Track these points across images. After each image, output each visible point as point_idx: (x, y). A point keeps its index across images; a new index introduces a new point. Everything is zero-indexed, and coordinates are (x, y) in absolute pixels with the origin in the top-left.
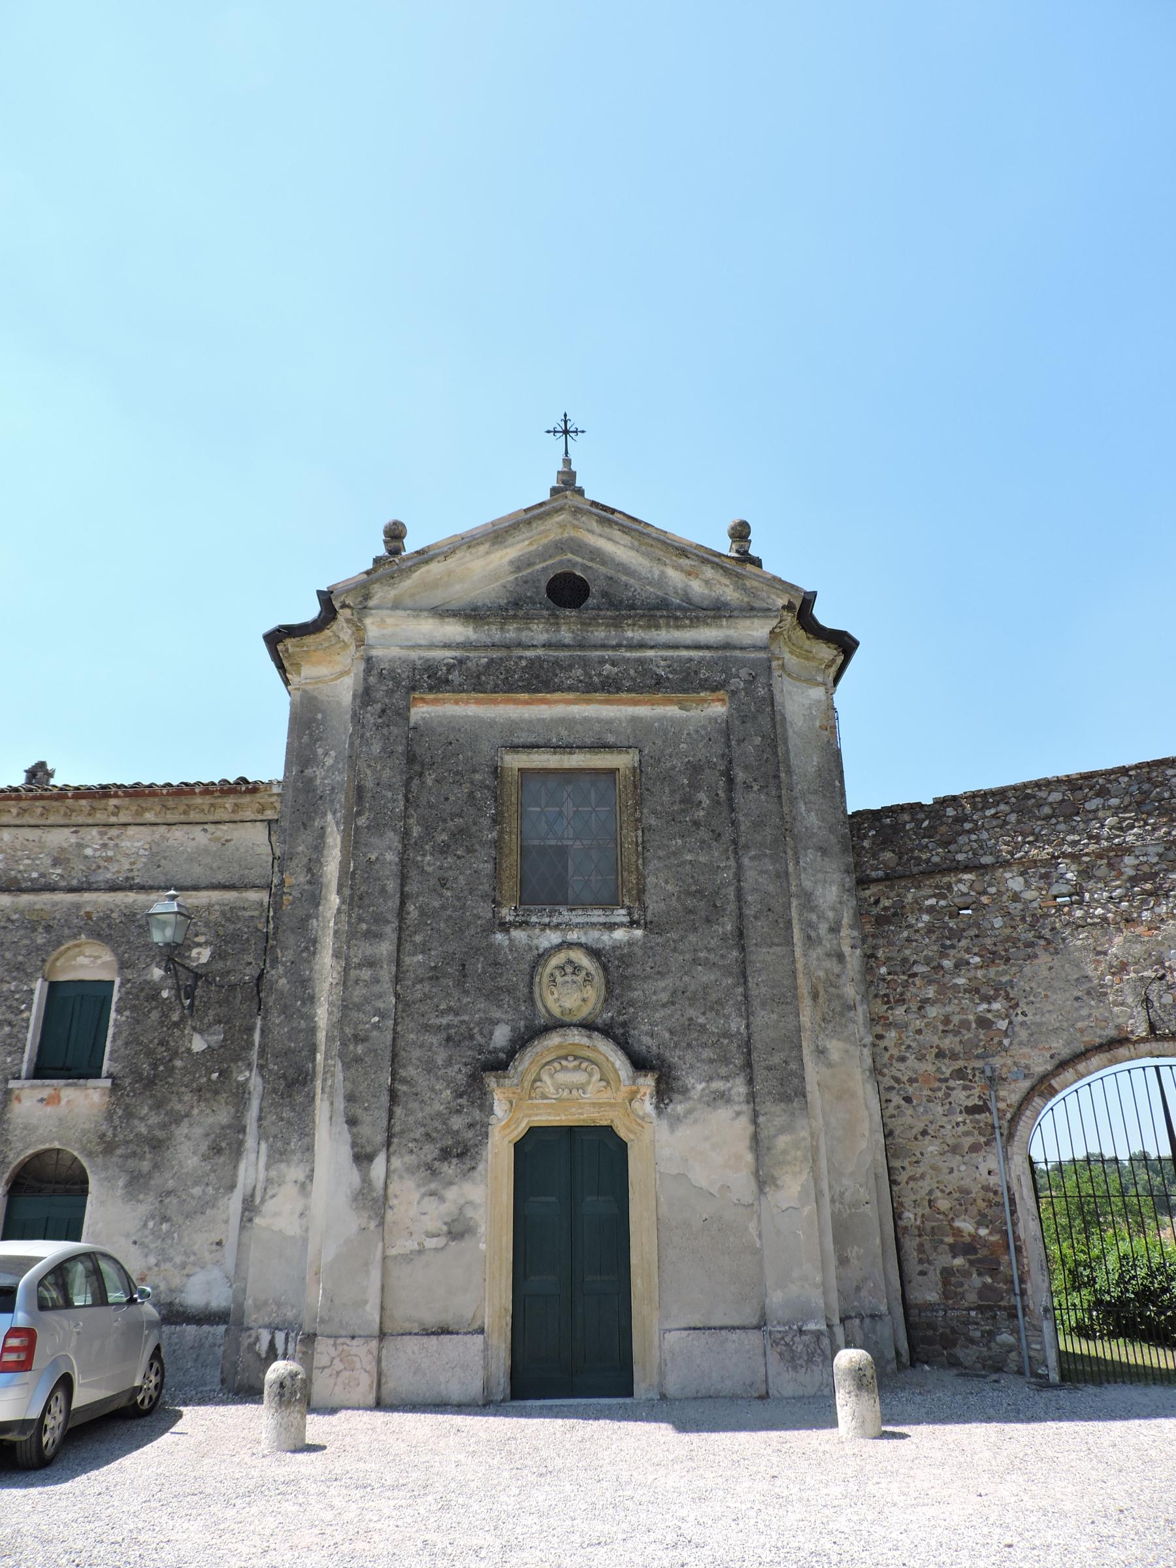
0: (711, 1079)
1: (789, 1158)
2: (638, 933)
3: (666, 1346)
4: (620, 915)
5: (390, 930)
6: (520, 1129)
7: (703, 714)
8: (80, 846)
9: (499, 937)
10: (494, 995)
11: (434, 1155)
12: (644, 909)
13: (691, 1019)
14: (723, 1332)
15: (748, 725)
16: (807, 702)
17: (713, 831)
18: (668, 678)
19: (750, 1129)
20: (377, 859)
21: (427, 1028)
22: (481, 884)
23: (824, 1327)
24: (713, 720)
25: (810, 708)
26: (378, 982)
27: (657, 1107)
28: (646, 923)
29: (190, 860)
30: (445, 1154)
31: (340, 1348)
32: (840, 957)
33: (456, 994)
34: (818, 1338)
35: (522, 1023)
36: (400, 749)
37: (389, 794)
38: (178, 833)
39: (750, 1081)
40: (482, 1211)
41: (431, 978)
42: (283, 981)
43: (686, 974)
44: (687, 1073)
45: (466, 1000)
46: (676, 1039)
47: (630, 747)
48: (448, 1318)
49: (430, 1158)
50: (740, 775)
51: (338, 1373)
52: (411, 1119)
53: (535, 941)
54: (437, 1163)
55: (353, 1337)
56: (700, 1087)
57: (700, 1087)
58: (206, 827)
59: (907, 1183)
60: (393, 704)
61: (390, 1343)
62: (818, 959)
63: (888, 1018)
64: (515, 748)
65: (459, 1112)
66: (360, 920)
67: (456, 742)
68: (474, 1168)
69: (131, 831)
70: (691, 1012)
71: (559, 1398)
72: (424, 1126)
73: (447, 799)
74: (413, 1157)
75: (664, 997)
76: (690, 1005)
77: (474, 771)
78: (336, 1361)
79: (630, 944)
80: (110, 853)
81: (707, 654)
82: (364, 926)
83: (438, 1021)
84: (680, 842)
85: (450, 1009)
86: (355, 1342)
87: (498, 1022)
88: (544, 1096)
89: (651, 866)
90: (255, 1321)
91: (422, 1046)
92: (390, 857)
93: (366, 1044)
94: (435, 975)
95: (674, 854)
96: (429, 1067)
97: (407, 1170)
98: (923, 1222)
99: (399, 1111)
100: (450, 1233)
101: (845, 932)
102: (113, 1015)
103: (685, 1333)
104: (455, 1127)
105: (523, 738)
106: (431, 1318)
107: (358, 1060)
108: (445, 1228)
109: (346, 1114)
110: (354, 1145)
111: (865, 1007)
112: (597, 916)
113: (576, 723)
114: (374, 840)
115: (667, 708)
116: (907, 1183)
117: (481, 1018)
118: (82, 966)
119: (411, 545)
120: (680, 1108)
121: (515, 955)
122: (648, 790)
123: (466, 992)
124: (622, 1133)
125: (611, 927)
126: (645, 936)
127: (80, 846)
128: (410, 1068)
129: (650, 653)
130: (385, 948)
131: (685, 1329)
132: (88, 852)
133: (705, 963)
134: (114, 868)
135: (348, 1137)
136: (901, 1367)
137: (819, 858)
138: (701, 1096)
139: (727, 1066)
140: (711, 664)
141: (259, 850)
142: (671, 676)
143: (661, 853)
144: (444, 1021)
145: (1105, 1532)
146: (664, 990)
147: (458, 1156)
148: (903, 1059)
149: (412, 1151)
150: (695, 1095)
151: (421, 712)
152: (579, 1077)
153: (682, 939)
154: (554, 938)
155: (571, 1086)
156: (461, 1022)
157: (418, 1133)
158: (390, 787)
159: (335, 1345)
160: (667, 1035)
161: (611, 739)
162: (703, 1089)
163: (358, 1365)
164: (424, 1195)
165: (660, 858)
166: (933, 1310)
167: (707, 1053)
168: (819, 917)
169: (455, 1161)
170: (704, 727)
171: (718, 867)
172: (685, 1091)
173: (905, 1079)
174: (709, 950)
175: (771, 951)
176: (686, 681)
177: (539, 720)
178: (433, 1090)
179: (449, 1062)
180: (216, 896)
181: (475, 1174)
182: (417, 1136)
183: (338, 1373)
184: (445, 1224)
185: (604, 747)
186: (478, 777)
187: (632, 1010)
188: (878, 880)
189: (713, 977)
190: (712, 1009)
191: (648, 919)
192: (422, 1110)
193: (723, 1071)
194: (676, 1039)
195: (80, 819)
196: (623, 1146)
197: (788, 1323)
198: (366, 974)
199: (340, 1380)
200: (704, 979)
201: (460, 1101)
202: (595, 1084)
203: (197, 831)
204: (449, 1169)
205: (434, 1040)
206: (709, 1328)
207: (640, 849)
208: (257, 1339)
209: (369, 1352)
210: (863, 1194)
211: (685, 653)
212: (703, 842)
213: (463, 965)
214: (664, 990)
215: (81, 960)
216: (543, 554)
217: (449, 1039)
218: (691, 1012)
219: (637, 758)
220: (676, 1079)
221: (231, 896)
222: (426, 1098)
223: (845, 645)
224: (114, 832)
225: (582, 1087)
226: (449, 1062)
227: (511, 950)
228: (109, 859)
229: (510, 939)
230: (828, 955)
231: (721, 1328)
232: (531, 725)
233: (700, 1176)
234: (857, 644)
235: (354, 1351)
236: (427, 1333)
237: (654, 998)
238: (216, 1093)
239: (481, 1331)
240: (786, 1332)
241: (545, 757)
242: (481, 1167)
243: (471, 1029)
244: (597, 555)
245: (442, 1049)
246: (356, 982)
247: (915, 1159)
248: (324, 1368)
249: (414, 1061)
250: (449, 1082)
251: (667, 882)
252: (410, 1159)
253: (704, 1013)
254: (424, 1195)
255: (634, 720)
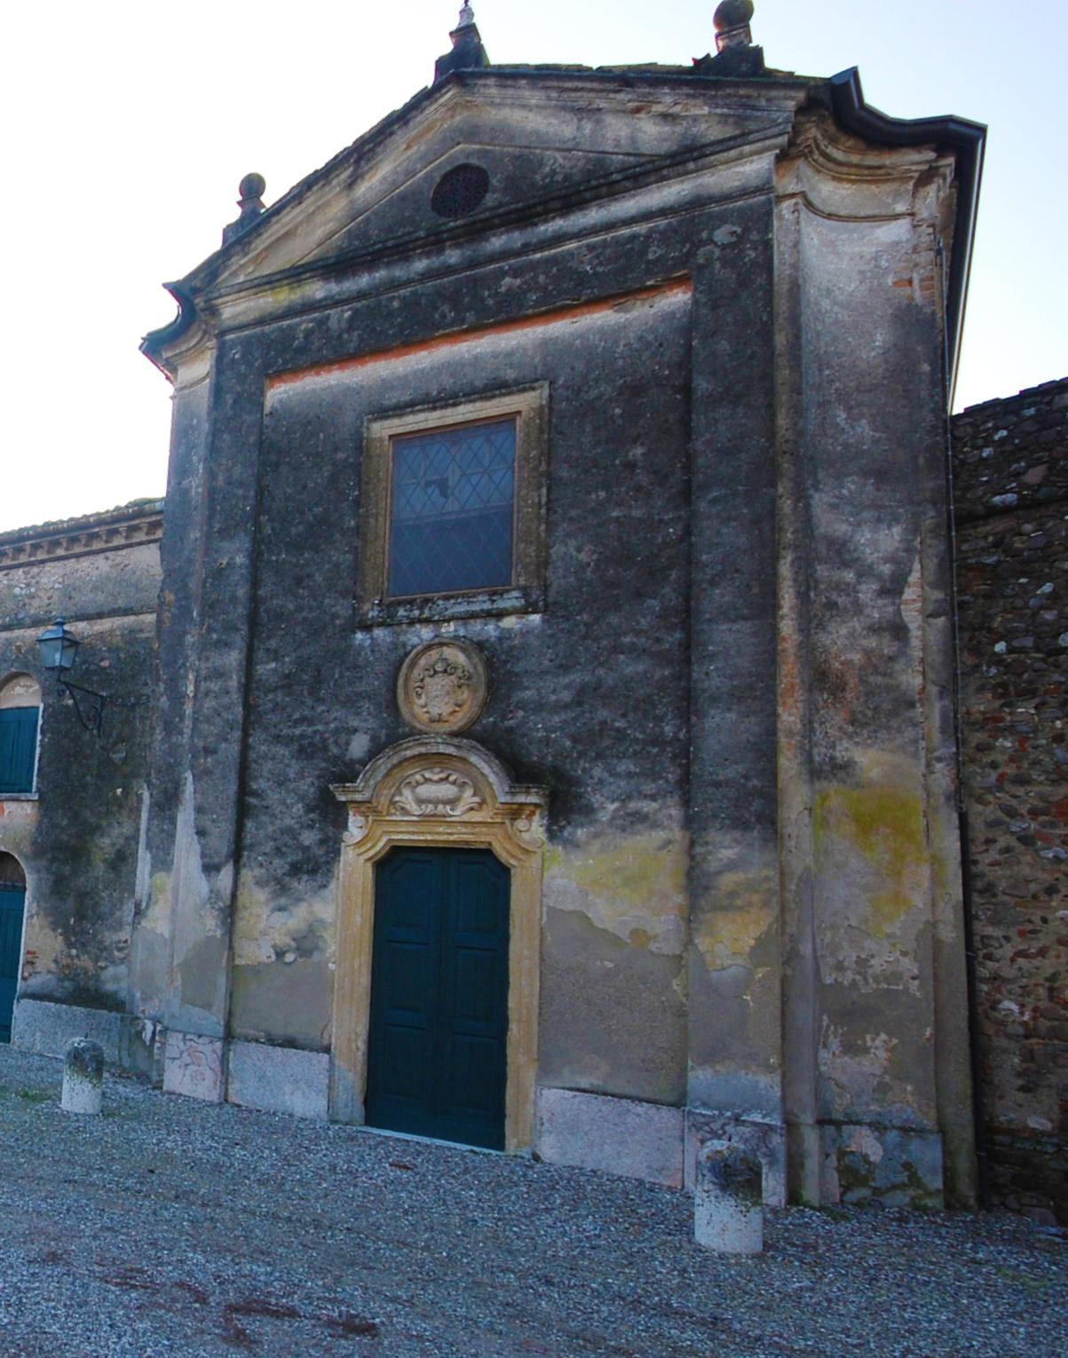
0: (629, 797)
1: (739, 902)
2: (536, 618)
3: (542, 1103)
4: (512, 600)
5: (239, 640)
6: (377, 848)
7: (652, 311)
8: (10, 587)
9: (359, 636)
10: (351, 703)
11: (284, 871)
12: (546, 588)
13: (603, 723)
14: (624, 1102)
15: (721, 311)
16: (869, 251)
17: (655, 472)
18: (596, 274)
19: (684, 862)
20: (228, 564)
21: (278, 738)
22: (340, 578)
23: (776, 1121)
24: (668, 317)
25: (876, 258)
26: (228, 692)
27: (549, 830)
28: (546, 606)
29: (95, 589)
30: (295, 870)
31: (189, 1043)
32: (898, 630)
33: (310, 702)
34: (765, 1134)
35: (384, 731)
36: (252, 439)
37: (240, 492)
38: (85, 563)
39: (686, 802)
40: (331, 931)
41: (282, 687)
42: (164, 699)
43: (601, 664)
44: (594, 790)
45: (320, 709)
46: (580, 747)
47: (537, 380)
48: (292, 1031)
49: (280, 872)
50: (702, 385)
51: (187, 1065)
52: (262, 833)
53: (402, 638)
54: (287, 879)
55: (200, 1036)
56: (612, 807)
57: (612, 807)
58: (108, 554)
59: (1013, 960)
60: (245, 391)
61: (238, 1048)
62: (852, 634)
63: (1002, 720)
64: (384, 413)
65: (311, 827)
66: (210, 630)
67: (310, 420)
68: (325, 886)
69: (48, 567)
70: (603, 714)
71: (455, 1141)
72: (275, 840)
73: (305, 487)
74: (263, 871)
75: (566, 696)
76: (604, 705)
77: (336, 449)
78: (185, 1054)
79: (524, 633)
80: (33, 590)
81: (662, 223)
82: (215, 636)
83: (290, 732)
84: (602, 494)
85: (303, 720)
86: (201, 1040)
87: (355, 731)
88: (405, 811)
89: (560, 532)
90: (143, 1012)
91: (273, 758)
92: (240, 559)
93: (215, 757)
94: (288, 682)
95: (592, 511)
96: (281, 782)
97: (257, 883)
98: (1034, 1018)
99: (249, 824)
100: (298, 949)
101: (910, 593)
102: (39, 737)
103: (569, 1094)
104: (307, 843)
105: (392, 398)
106: (279, 1031)
107: (208, 772)
108: (293, 944)
109: (197, 827)
110: (203, 855)
111: (946, 702)
112: (481, 604)
113: (463, 366)
114: (225, 544)
115: (596, 316)
116: (1013, 960)
117: (337, 728)
118: (19, 695)
119: (269, 199)
120: (581, 833)
121: (378, 655)
122: (561, 433)
123: (321, 700)
124: (503, 856)
125: (500, 615)
126: (544, 621)
127: (10, 587)
128: (261, 781)
129: (572, 245)
130: (234, 658)
131: (571, 1089)
132: (17, 591)
133: (631, 649)
134: (36, 603)
135: (197, 848)
136: (953, 1201)
137: (869, 488)
138: (613, 818)
139: (654, 781)
140: (664, 236)
141: (152, 571)
142: (600, 269)
143: (573, 513)
144: (297, 732)
145: (124, 1340)
146: (566, 687)
147: (308, 872)
148: (1022, 781)
149: (261, 865)
150: (604, 816)
151: (278, 393)
152: (447, 790)
153: (597, 620)
154: (426, 633)
155: (445, 804)
156: (315, 732)
157: (269, 847)
158: (241, 484)
159: (184, 1040)
160: (568, 743)
161: (511, 374)
162: (617, 810)
163: (204, 1062)
164: (273, 911)
165: (571, 519)
166: (1039, 1142)
167: (625, 766)
168: (860, 575)
169: (305, 877)
170: (652, 330)
171: (661, 521)
172: (589, 811)
173: (1024, 809)
174: (638, 633)
175: (735, 627)
176: (621, 275)
177: (415, 373)
178: (283, 803)
179: (301, 775)
180: (118, 622)
181: (326, 892)
182: (267, 850)
183: (187, 1065)
184: (294, 940)
185: (499, 387)
186: (341, 455)
187: (521, 713)
188: (1006, 510)
189: (641, 668)
190: (636, 709)
191: (550, 600)
192: (272, 823)
193: (649, 788)
194: (580, 747)
195: (9, 562)
196: (504, 872)
197: (721, 1108)
198: (215, 686)
199: (188, 1072)
200: (629, 670)
201: (312, 816)
202: (468, 797)
203: (100, 559)
204: (300, 885)
205: (281, 750)
206: (605, 1094)
207: (543, 511)
208: (144, 1028)
209: (214, 1051)
210: (909, 966)
211: (626, 231)
212: (638, 489)
213: (319, 671)
214: (566, 687)
215: (18, 690)
216: (426, 160)
217: (301, 750)
218: (603, 714)
219: (546, 392)
220: (581, 796)
221: (129, 620)
222: (277, 812)
223: (956, 144)
224: (35, 570)
225: (453, 802)
226: (301, 775)
227: (373, 651)
228: (32, 597)
229: (372, 638)
230: (874, 629)
231: (621, 1097)
232: (404, 381)
233: (605, 914)
234: (981, 130)
235: (200, 1048)
236: (272, 1041)
237: (553, 698)
238: (121, 806)
239: (327, 1050)
240: (713, 1116)
241: (422, 416)
242: (332, 886)
243: (326, 740)
244: (501, 132)
245: (294, 761)
246: (207, 694)
247: (1030, 927)
248: (174, 1059)
249: (265, 773)
250: (301, 798)
251: (579, 550)
252: (258, 872)
253: (624, 715)
254: (273, 911)
255: (545, 342)
